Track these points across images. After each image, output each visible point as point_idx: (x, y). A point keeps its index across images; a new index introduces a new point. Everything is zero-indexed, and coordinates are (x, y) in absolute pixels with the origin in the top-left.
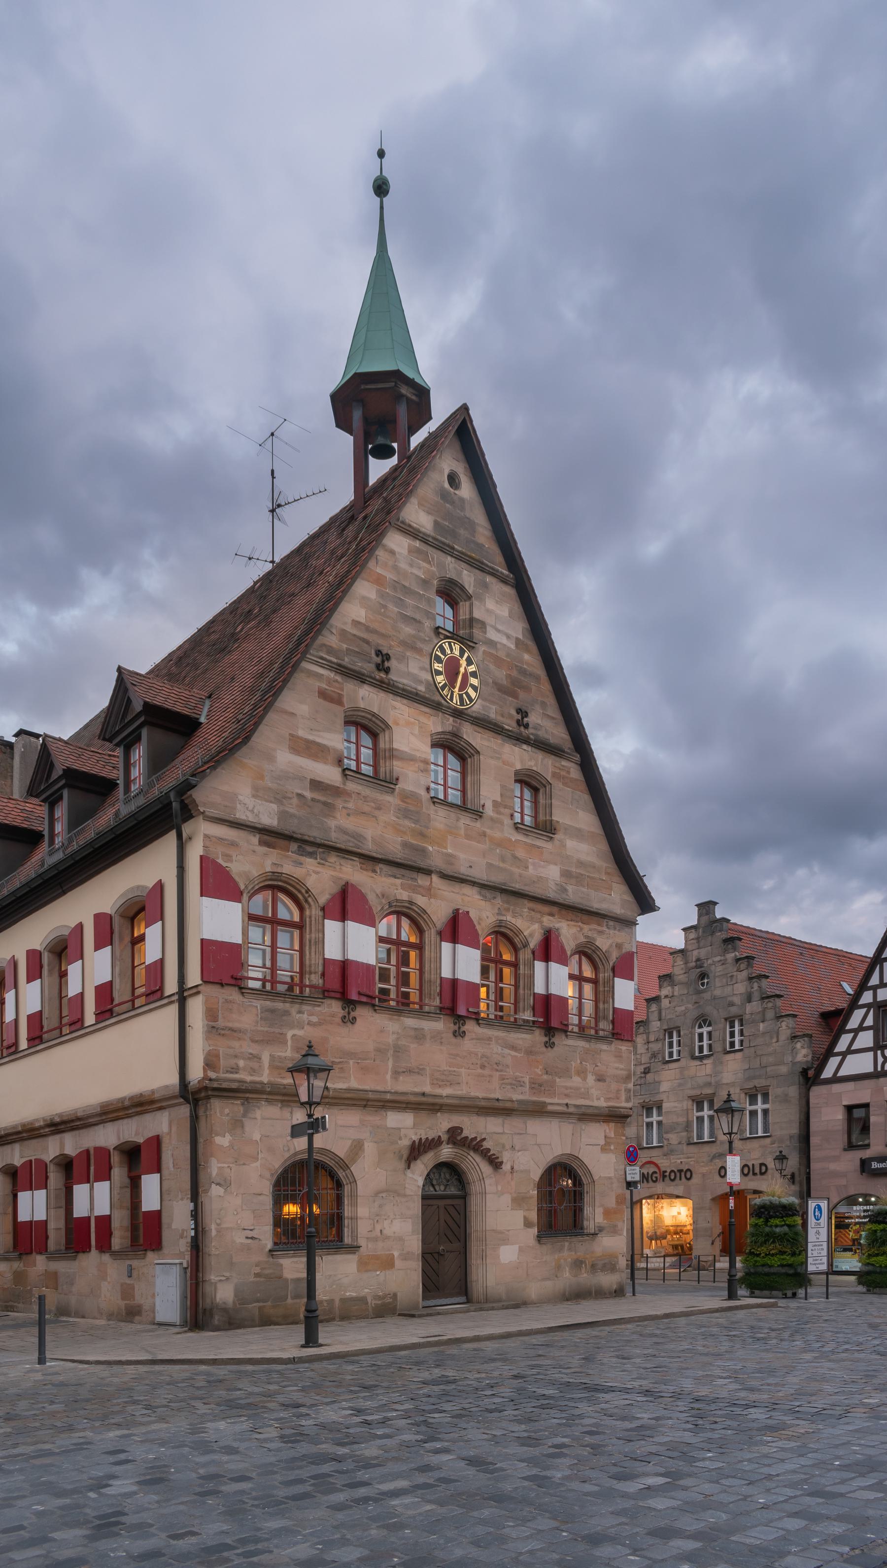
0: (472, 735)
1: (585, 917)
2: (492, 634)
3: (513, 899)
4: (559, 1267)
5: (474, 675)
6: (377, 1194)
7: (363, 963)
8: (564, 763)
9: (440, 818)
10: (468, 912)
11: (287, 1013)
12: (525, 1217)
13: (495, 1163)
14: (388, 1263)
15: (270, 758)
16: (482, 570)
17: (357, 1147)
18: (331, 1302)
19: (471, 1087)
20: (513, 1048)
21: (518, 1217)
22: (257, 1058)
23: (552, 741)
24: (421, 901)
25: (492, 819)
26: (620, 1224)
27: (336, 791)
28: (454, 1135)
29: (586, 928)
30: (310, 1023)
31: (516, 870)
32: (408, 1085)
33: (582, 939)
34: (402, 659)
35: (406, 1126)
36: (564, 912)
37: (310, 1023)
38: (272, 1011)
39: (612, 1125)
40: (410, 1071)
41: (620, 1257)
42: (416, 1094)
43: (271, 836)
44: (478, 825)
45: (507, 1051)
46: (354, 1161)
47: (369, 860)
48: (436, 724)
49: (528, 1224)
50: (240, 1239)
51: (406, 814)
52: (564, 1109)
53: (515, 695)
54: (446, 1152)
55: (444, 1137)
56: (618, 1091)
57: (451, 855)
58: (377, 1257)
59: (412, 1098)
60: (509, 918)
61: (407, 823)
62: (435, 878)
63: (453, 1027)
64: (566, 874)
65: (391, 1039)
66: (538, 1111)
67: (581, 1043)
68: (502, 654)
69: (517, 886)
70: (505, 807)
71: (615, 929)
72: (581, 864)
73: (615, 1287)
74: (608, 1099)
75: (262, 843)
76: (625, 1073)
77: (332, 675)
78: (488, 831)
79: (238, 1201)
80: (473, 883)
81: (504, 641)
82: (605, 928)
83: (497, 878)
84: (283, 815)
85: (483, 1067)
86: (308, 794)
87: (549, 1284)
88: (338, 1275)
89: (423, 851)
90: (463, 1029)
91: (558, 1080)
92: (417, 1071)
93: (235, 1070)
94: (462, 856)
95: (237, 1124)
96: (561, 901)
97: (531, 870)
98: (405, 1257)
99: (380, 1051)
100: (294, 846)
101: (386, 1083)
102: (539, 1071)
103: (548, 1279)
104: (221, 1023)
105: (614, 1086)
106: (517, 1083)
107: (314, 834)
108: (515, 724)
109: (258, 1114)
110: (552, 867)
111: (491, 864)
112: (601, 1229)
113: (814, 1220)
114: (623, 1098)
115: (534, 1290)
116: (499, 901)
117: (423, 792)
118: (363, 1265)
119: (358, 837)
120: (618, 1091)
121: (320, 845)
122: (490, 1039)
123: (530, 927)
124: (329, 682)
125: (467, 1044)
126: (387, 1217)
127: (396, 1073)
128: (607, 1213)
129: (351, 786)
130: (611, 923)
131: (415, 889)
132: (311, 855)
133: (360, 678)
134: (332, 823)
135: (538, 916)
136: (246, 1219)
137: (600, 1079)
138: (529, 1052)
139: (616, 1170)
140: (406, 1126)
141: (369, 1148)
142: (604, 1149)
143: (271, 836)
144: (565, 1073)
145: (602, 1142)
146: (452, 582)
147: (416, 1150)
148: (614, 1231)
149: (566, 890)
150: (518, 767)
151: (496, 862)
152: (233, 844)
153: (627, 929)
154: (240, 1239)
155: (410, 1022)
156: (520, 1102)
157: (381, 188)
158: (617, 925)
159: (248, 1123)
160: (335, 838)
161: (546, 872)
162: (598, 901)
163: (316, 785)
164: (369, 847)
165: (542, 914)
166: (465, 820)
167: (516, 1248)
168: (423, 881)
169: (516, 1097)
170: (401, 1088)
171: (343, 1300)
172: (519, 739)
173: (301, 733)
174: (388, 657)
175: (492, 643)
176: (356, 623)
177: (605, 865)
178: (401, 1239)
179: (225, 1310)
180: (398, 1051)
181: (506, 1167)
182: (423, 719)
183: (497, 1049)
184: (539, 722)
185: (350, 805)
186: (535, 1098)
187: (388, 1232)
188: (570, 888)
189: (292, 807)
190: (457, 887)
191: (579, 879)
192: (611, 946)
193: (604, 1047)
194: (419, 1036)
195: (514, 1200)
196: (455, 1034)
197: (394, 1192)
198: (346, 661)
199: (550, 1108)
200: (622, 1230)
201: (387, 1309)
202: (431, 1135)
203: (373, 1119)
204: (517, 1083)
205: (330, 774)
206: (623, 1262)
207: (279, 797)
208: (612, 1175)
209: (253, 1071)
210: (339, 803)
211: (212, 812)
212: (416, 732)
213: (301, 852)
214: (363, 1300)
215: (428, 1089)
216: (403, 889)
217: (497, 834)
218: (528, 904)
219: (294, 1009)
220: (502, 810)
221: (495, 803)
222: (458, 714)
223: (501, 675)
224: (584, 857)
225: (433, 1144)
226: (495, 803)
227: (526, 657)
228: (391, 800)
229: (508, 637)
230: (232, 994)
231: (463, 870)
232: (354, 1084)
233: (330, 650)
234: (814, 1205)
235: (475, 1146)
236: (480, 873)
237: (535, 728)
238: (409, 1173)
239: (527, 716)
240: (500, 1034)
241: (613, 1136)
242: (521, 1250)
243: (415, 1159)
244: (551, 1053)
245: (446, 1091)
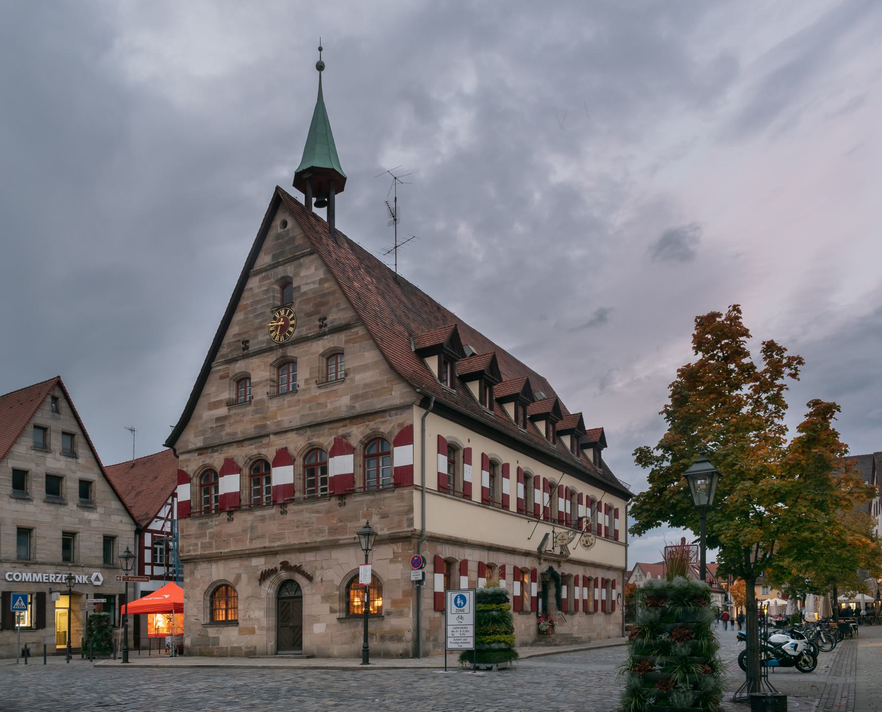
0: (292, 352)
1: (371, 417)
2: (304, 289)
3: (317, 428)
4: (354, 637)
5: (292, 319)
6: (247, 598)
7: (232, 493)
8: (353, 330)
9: (273, 405)
10: (286, 448)
11: (207, 523)
12: (331, 608)
13: (310, 578)
14: (252, 631)
15: (200, 417)
16: (298, 259)
17: (238, 577)
18: (227, 648)
19: (291, 539)
20: (317, 512)
21: (326, 607)
22: (196, 544)
23: (343, 322)
24: (264, 451)
25: (304, 390)
26: (406, 610)
27: (225, 418)
28: (285, 566)
29: (372, 425)
30: (216, 525)
31: (319, 411)
32: (257, 545)
33: (368, 431)
34: (256, 336)
35: (260, 564)
36: (354, 421)
37: (216, 525)
38: (202, 524)
39: (400, 544)
40: (258, 537)
41: (406, 632)
42: (260, 548)
43: (201, 451)
44: (296, 397)
45: (313, 515)
46: (237, 584)
47: (240, 442)
48: (272, 358)
49: (332, 611)
50: (193, 620)
51: (256, 412)
52: (353, 541)
53: (318, 312)
54: (284, 575)
55: (279, 567)
56: (400, 521)
57: (280, 421)
58: (247, 628)
59: (258, 550)
60: (315, 440)
61: (257, 416)
62: (271, 436)
63: (280, 510)
64: (355, 398)
65: (249, 524)
66: (334, 545)
67: (367, 498)
68: (310, 295)
69: (319, 420)
70: (312, 379)
71: (397, 414)
72: (366, 385)
73: (401, 652)
74: (388, 529)
75: (199, 454)
76: (406, 508)
77: (224, 366)
78: (301, 398)
79: (192, 604)
80: (292, 430)
81: (312, 286)
82: (388, 418)
83: (306, 421)
84: (205, 440)
85: (298, 527)
86: (214, 425)
87: (347, 647)
88: (229, 637)
89: (264, 426)
90: (287, 509)
91: (349, 524)
92: (263, 536)
93: (189, 551)
94: (285, 418)
95: (192, 573)
96: (351, 415)
97: (329, 407)
98: (261, 628)
99: (244, 531)
100: (210, 450)
101: (248, 545)
102: (334, 522)
103: (346, 643)
104: (185, 533)
105: (396, 518)
106: (321, 531)
107: (217, 442)
108: (317, 329)
109: (199, 567)
110: (344, 398)
111: (303, 415)
112: (389, 614)
113: (454, 608)
114: (405, 525)
115: (335, 650)
116: (309, 433)
117: (265, 397)
118: (241, 632)
119: (235, 434)
120: (400, 521)
121: (219, 445)
122: (302, 511)
123: (326, 440)
124: (224, 370)
125: (289, 517)
126: (256, 612)
127: (251, 540)
128: (394, 603)
129: (232, 412)
130: (393, 412)
131: (260, 447)
132: (216, 451)
133: (235, 360)
134: (223, 433)
135: (335, 430)
136: (195, 612)
137: (384, 516)
138: (328, 512)
139: (402, 574)
140: (260, 564)
141: (244, 577)
142: (392, 561)
143: (201, 451)
144: (356, 518)
145: (391, 556)
146: (282, 278)
147: (264, 576)
148: (401, 614)
149: (354, 407)
150: (321, 351)
151: (306, 412)
152: (189, 460)
153: (408, 411)
154: (193, 620)
155: (258, 513)
156: (321, 542)
157: (320, 67)
158: (399, 412)
159: (196, 572)
160: (225, 439)
161: (341, 402)
162: (378, 404)
163: (218, 419)
164: (240, 437)
165: (337, 428)
166: (288, 398)
167: (324, 625)
168: (265, 441)
169: (319, 539)
170: (253, 546)
171: (232, 648)
172: (319, 336)
173: (212, 400)
174: (248, 341)
175: (305, 293)
176: (234, 336)
177: (386, 377)
178: (258, 620)
179: (188, 648)
180: (253, 528)
181: (317, 579)
182: (266, 360)
183: (306, 515)
184: (335, 317)
185: (232, 421)
186: (331, 538)
187: (252, 616)
188: (357, 405)
189: (208, 435)
190: (284, 436)
191: (364, 396)
192: (393, 427)
193: (388, 495)
194: (263, 519)
195: (323, 598)
196: (282, 513)
197: (255, 597)
198: (230, 357)
199: (341, 542)
200: (408, 614)
201: (251, 653)
202: (271, 566)
203: (246, 563)
204: (321, 531)
205: (223, 411)
206: (409, 636)
207: (203, 433)
208: (399, 577)
209: (195, 550)
210: (227, 423)
211: (181, 451)
212: (263, 367)
213: (213, 451)
214: (240, 648)
215: (267, 544)
216: (255, 448)
217: (307, 396)
218: (327, 426)
219: (209, 521)
220: (310, 382)
221: (306, 381)
222: (282, 346)
223: (309, 308)
224: (368, 381)
225: (273, 571)
226: (306, 381)
227: (326, 285)
228: (250, 409)
229: (314, 283)
230: (188, 521)
231: (286, 425)
232: (233, 548)
233: (223, 356)
234: (454, 595)
235: (298, 569)
236: (297, 423)
237: (332, 322)
238: (263, 587)
239: (325, 319)
240: (309, 506)
241: (400, 551)
242: (327, 626)
243: (264, 580)
244: (343, 510)
245: (276, 544)
